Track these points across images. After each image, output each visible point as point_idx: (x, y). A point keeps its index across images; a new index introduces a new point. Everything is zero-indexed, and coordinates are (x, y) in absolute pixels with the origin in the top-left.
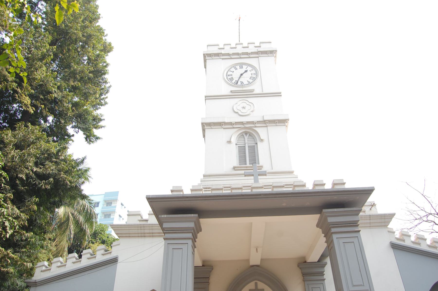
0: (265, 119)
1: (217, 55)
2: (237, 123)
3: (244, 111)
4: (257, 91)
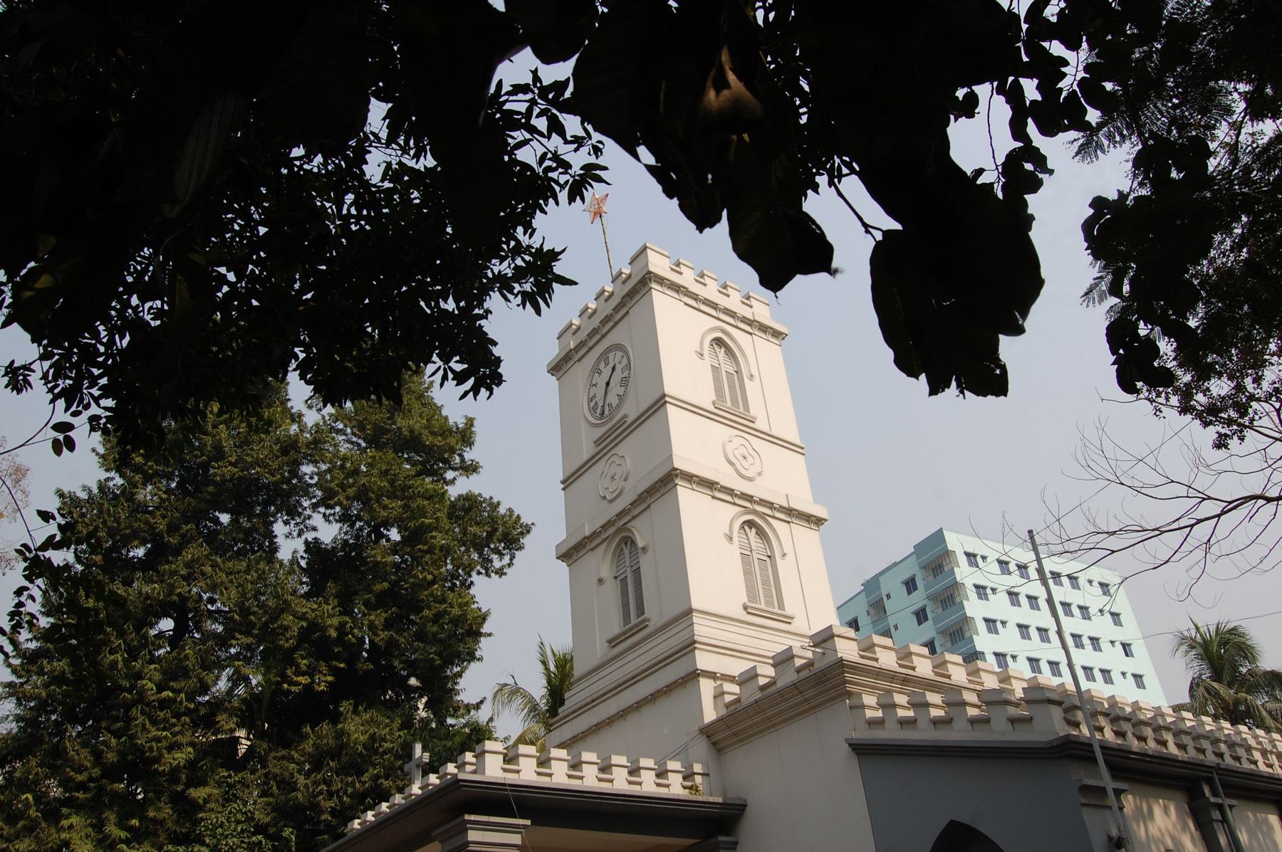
1: (676, 288)
3: (744, 463)
4: (761, 424)
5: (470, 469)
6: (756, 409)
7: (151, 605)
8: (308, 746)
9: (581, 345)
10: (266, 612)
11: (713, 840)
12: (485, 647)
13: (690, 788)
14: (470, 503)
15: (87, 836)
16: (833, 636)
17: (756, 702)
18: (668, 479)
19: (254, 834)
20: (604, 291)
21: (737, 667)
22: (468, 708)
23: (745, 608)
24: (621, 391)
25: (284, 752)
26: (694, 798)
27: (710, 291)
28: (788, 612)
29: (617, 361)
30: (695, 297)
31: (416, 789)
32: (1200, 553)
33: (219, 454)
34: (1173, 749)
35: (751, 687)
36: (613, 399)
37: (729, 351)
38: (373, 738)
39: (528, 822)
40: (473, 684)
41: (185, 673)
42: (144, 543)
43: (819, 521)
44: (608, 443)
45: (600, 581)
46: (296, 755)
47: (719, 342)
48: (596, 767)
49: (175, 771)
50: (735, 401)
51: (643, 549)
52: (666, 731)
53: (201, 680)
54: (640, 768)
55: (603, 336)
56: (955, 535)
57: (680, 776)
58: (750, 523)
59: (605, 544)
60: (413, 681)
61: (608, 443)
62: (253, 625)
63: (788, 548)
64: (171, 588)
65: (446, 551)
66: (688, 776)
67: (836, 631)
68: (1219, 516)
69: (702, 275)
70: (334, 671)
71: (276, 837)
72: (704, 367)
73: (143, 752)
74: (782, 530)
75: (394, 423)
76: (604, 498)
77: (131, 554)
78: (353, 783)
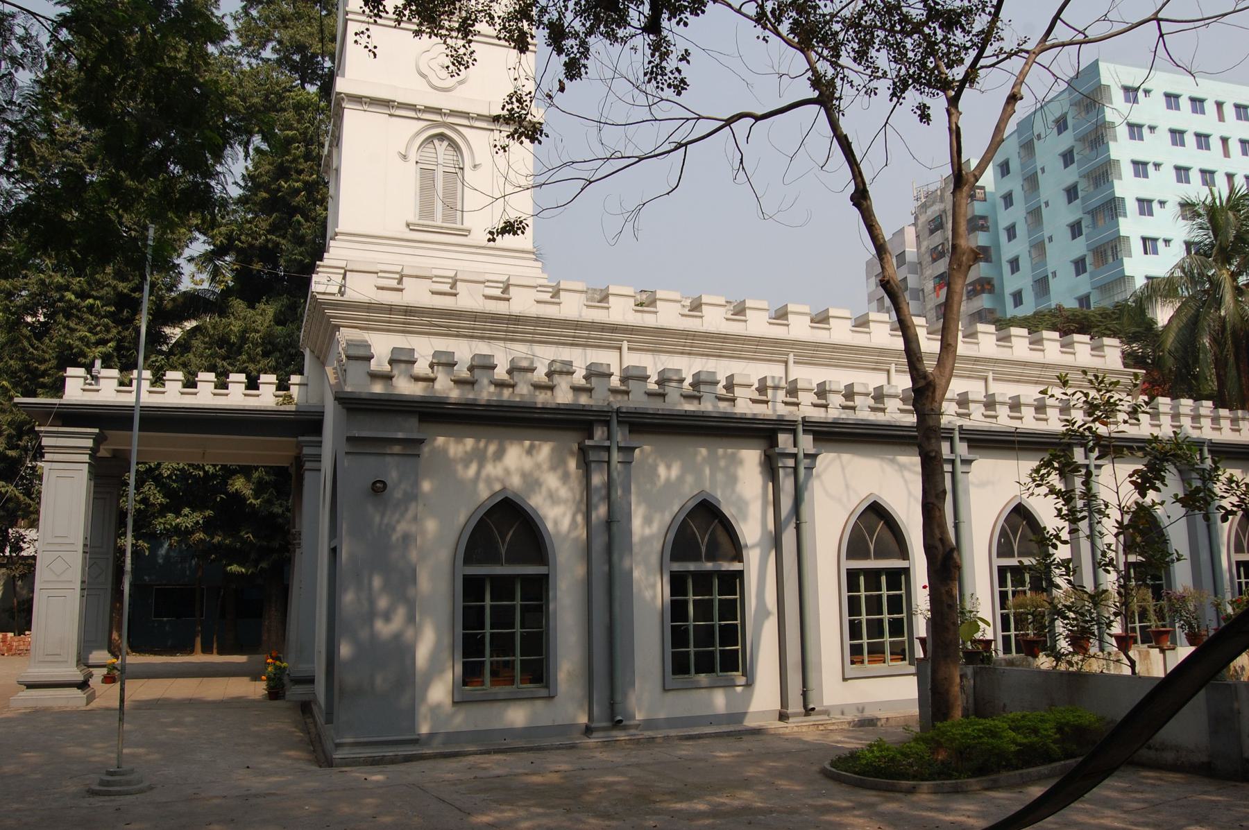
2: (428, 109)
28: (466, 225)
56: (1111, 66)
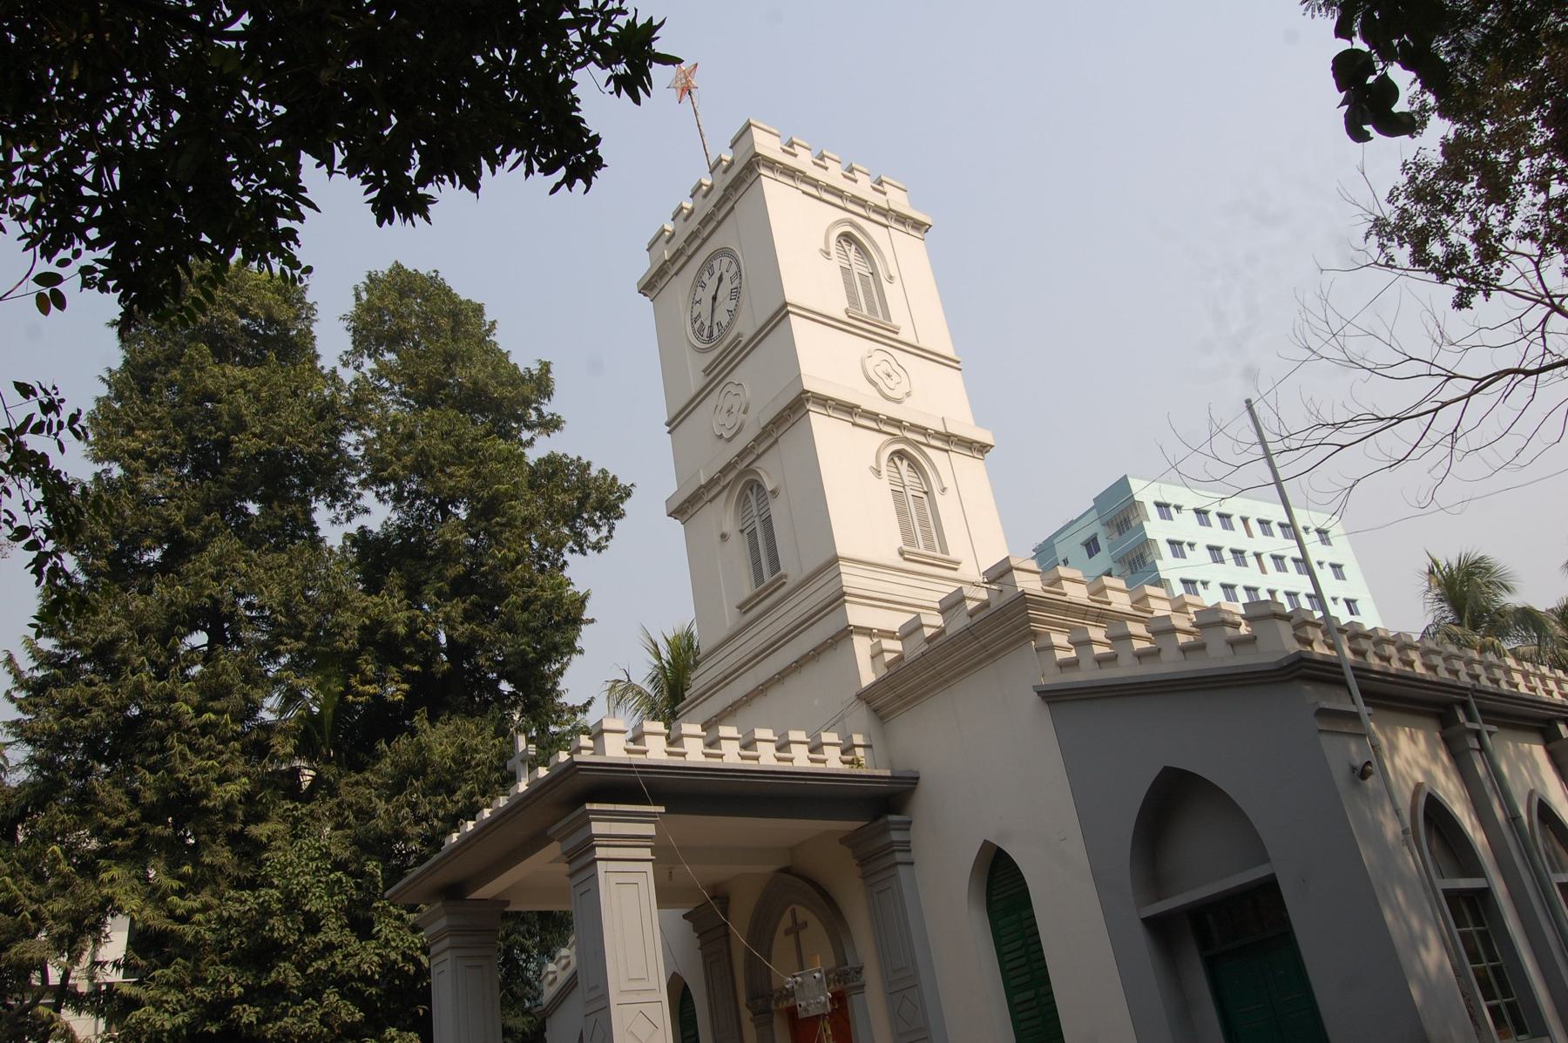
0: (951, 430)
1: (791, 173)
3: (888, 381)
4: (906, 335)
5: (551, 425)
6: (898, 316)
7: (176, 613)
8: (386, 765)
9: (678, 253)
10: (318, 610)
11: (882, 821)
12: (586, 637)
13: (851, 762)
14: (554, 467)
15: (133, 890)
16: (1011, 569)
17: (923, 654)
18: (799, 405)
19: (331, 872)
20: (701, 185)
21: (895, 621)
22: (574, 711)
23: (902, 553)
24: (731, 305)
25: (358, 777)
26: (856, 771)
27: (833, 175)
28: (953, 555)
29: (723, 269)
30: (814, 183)
31: (522, 786)
32: (1443, 450)
33: (239, 425)
34: (1419, 669)
35: (915, 640)
36: (722, 316)
37: (861, 249)
38: (462, 749)
39: (662, 809)
40: (579, 681)
41: (226, 690)
42: (159, 541)
43: (982, 448)
44: (718, 373)
45: (724, 536)
46: (371, 778)
47: (847, 238)
48: (737, 743)
49: (229, 804)
50: (872, 309)
51: (773, 492)
52: (816, 702)
53: (246, 697)
54: (789, 743)
55: (705, 240)
57: (837, 750)
58: (900, 454)
59: (725, 494)
60: (505, 687)
61: (718, 373)
62: (303, 626)
63: (948, 481)
64: (199, 588)
65: (530, 523)
66: (848, 749)
67: (1013, 562)
68: (1468, 396)
69: (822, 157)
70: (408, 677)
71: (361, 874)
72: (832, 269)
73: (187, 788)
74: (939, 460)
75: (452, 375)
76: (721, 436)
77: (146, 558)
78: (443, 803)
